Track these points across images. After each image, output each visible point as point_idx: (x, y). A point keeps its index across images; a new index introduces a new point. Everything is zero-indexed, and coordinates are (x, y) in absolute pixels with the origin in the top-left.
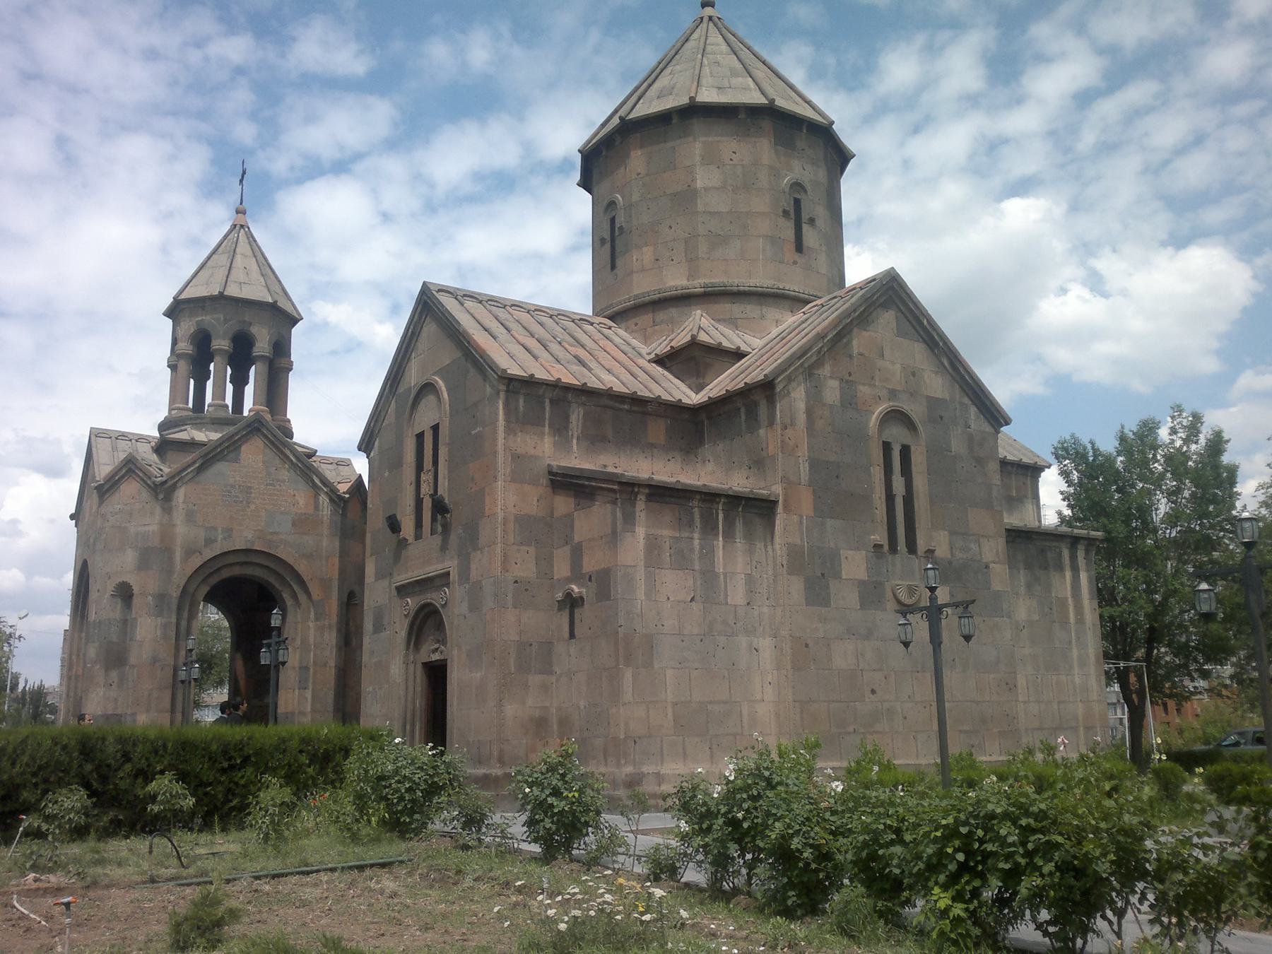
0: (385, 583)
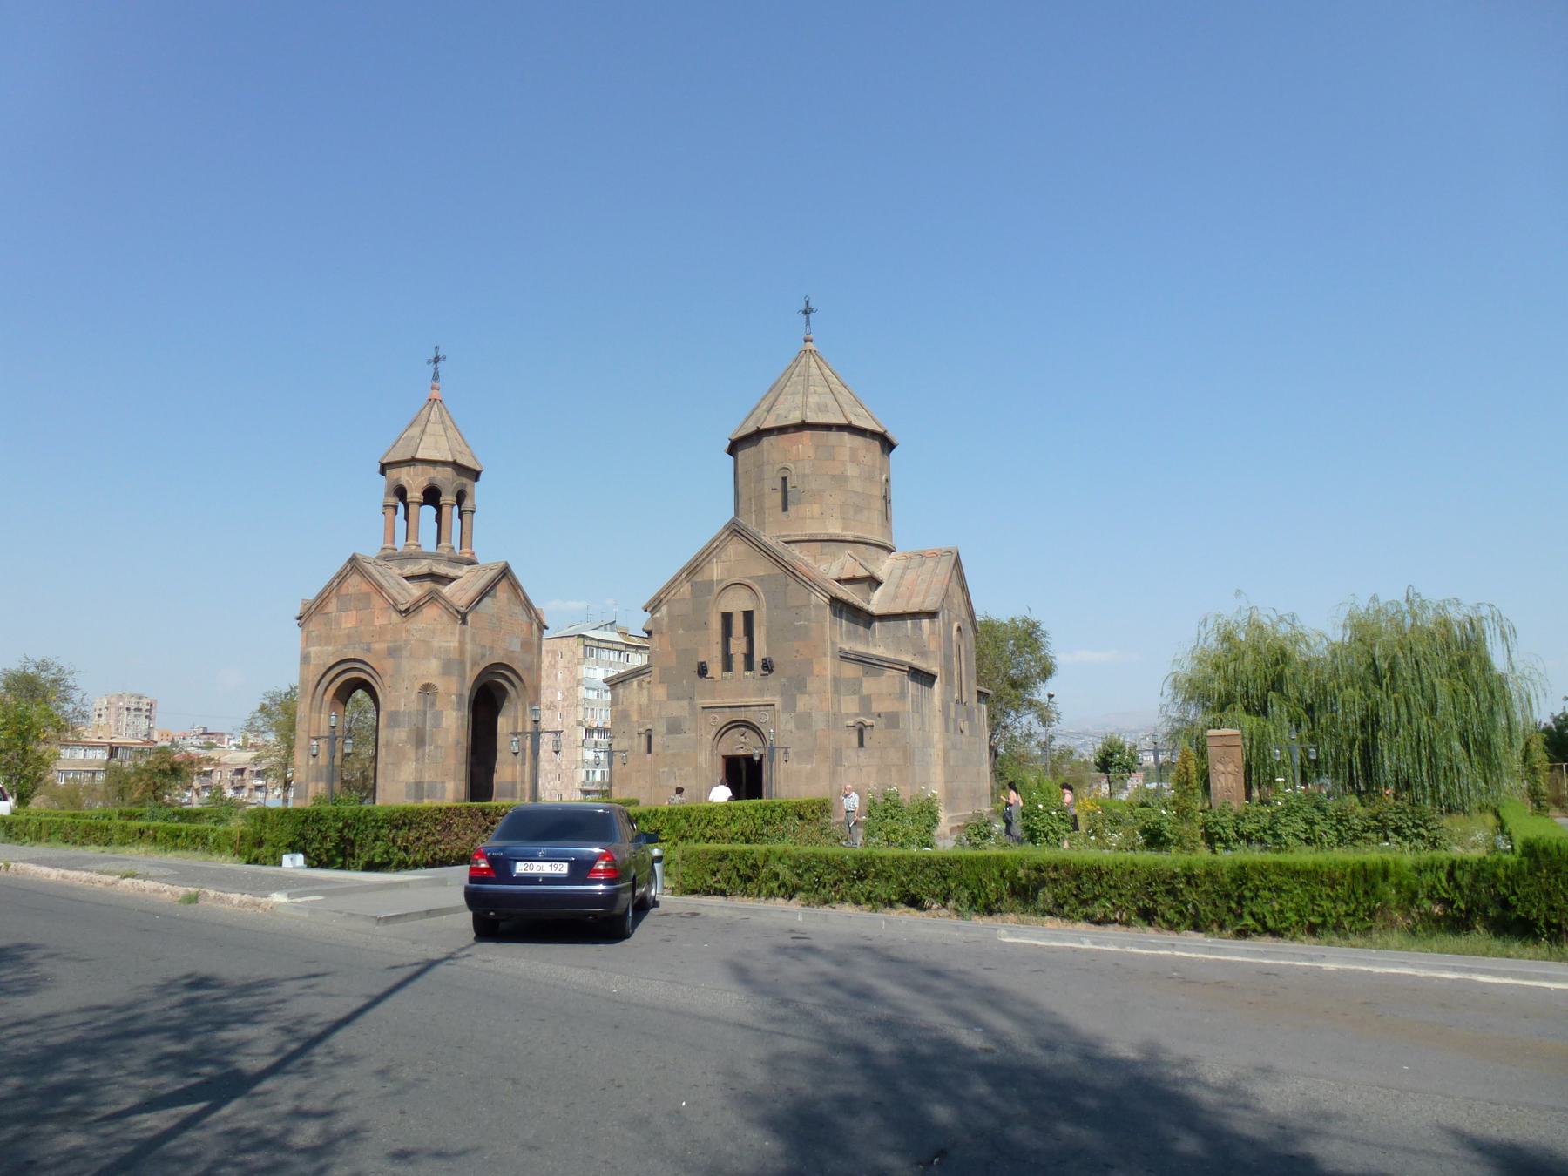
0: (685, 703)
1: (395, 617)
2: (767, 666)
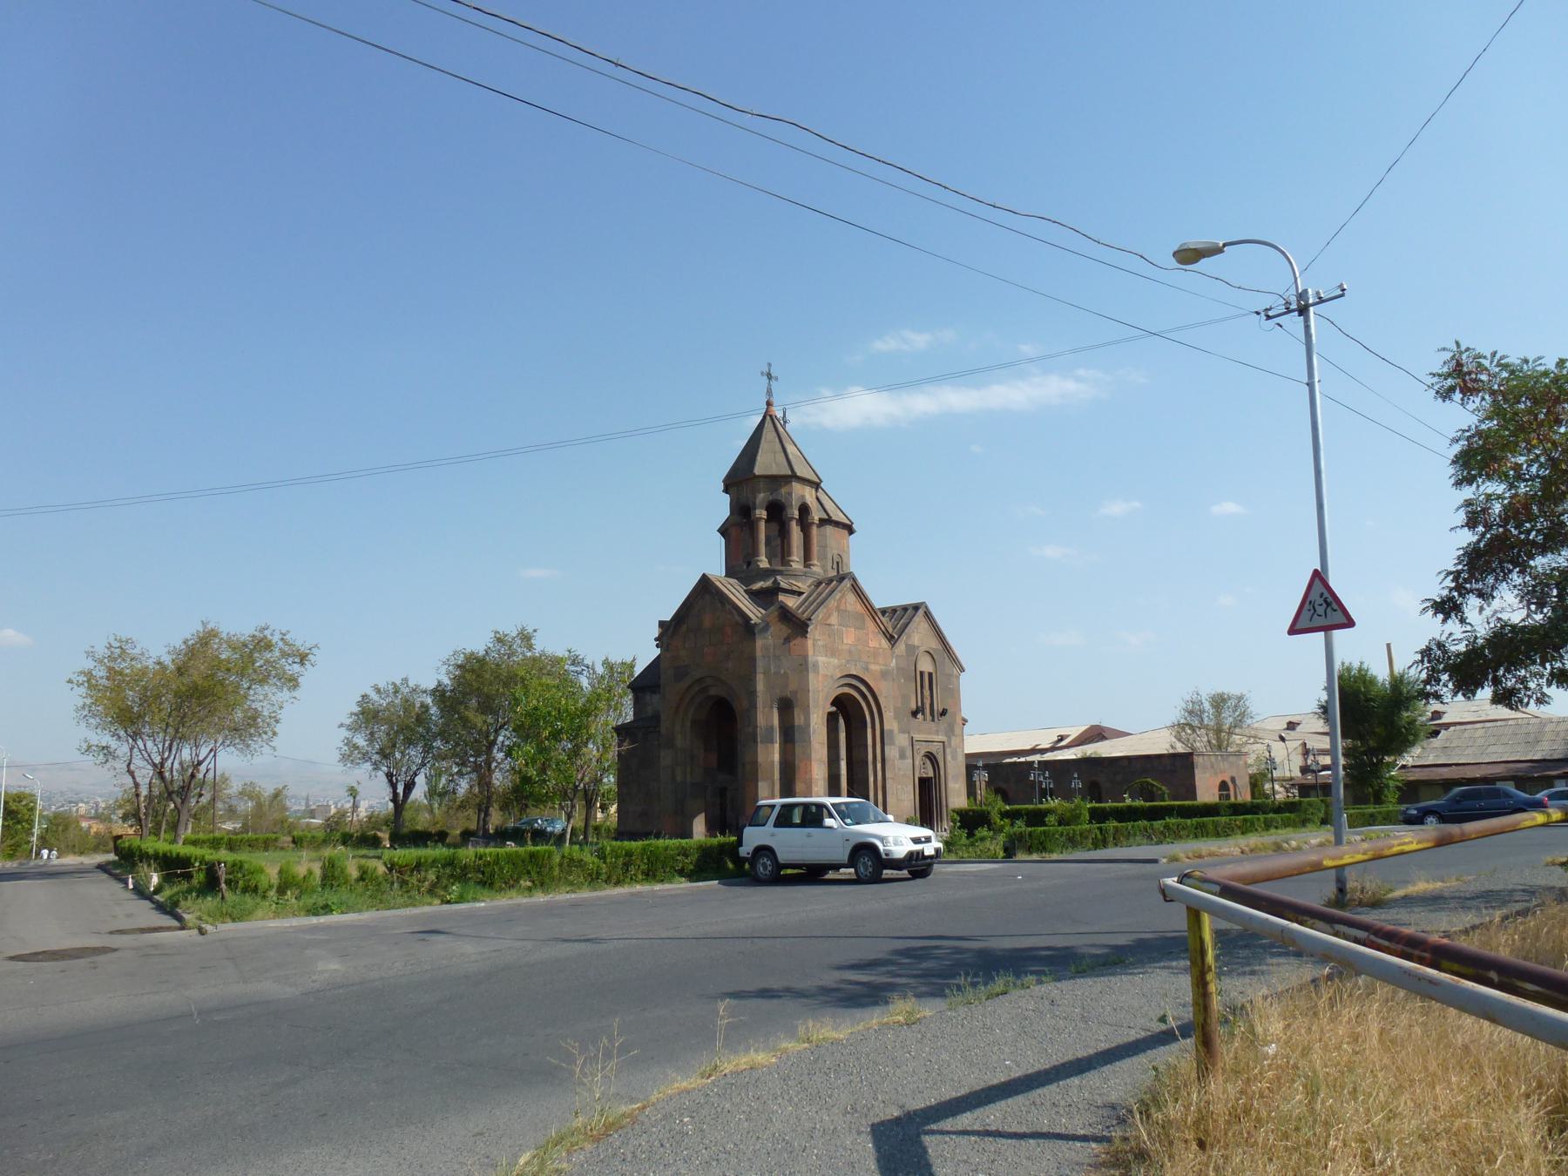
1: (885, 643)
2: (944, 713)
